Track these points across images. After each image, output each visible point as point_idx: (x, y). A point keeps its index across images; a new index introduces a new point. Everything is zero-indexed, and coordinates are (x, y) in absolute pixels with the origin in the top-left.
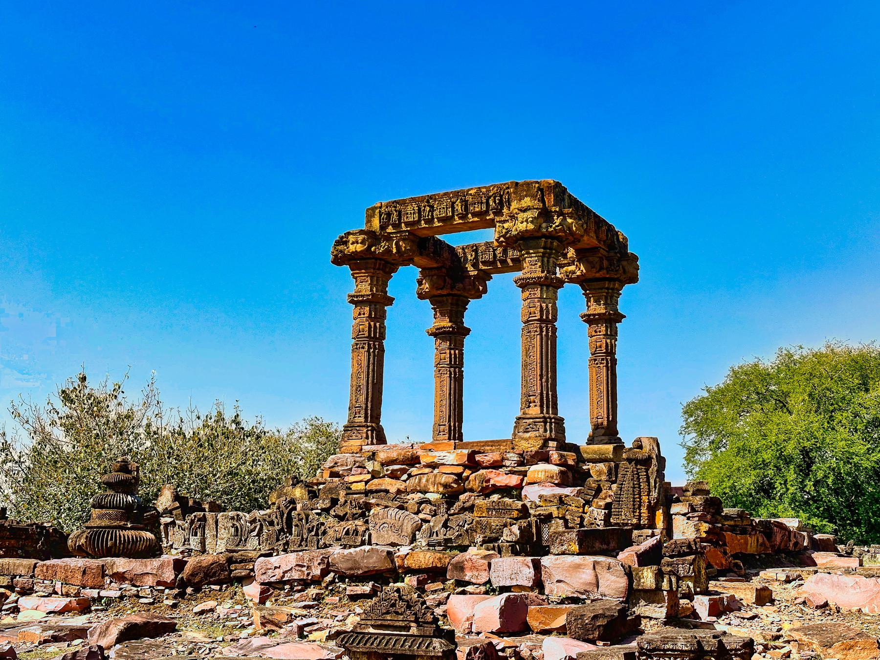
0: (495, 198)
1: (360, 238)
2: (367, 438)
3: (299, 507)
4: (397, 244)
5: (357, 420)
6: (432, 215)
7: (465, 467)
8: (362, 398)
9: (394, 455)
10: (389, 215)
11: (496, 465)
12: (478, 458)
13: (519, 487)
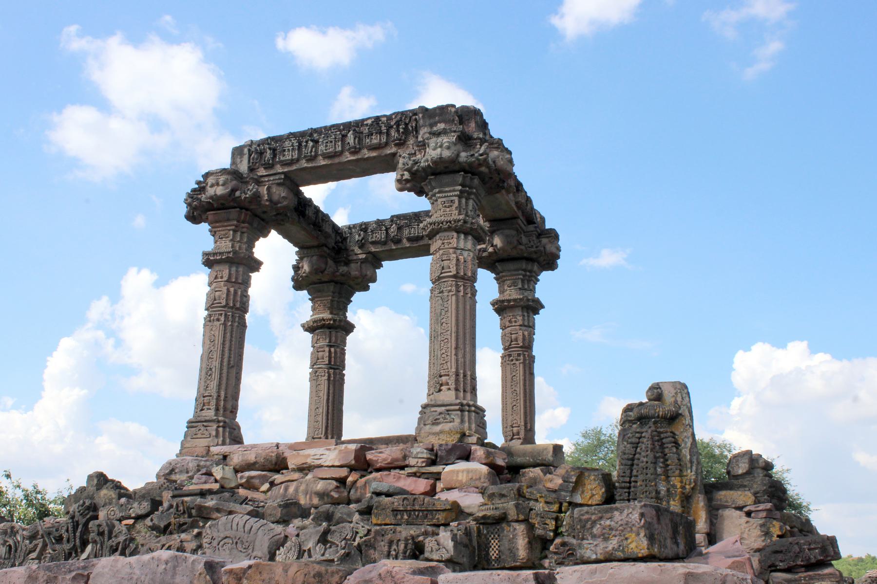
0: (398, 126)
1: (222, 179)
2: (217, 436)
3: (102, 514)
4: (269, 189)
5: (204, 413)
6: (316, 152)
7: (352, 469)
8: (213, 385)
9: (251, 458)
10: (261, 153)
11: (399, 466)
12: (370, 456)
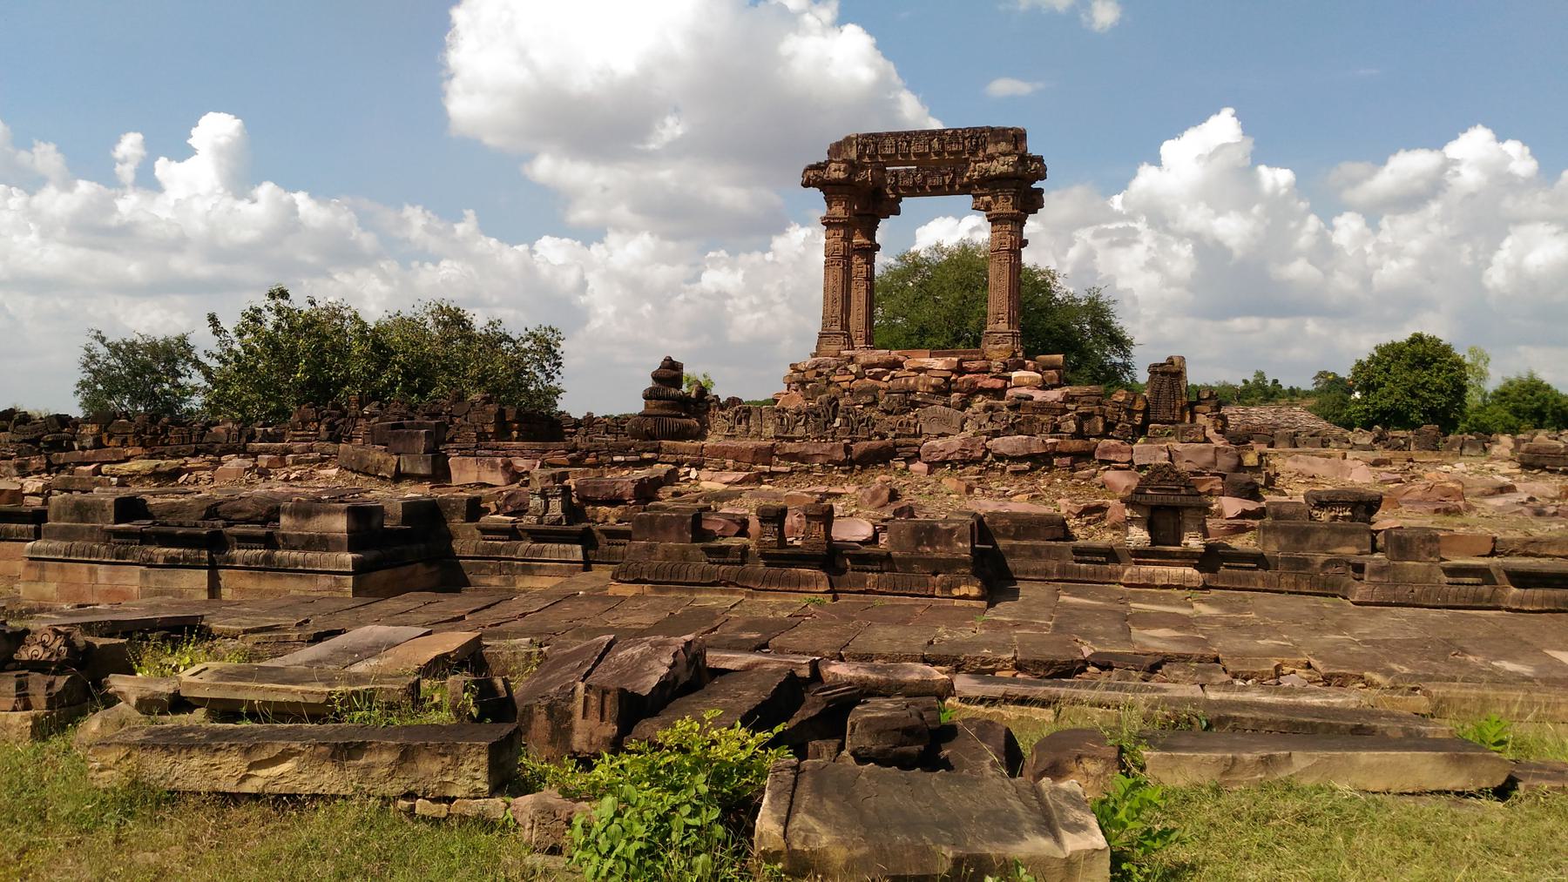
7: (953, 371)
8: (838, 309)
11: (986, 370)
13: (1005, 388)
